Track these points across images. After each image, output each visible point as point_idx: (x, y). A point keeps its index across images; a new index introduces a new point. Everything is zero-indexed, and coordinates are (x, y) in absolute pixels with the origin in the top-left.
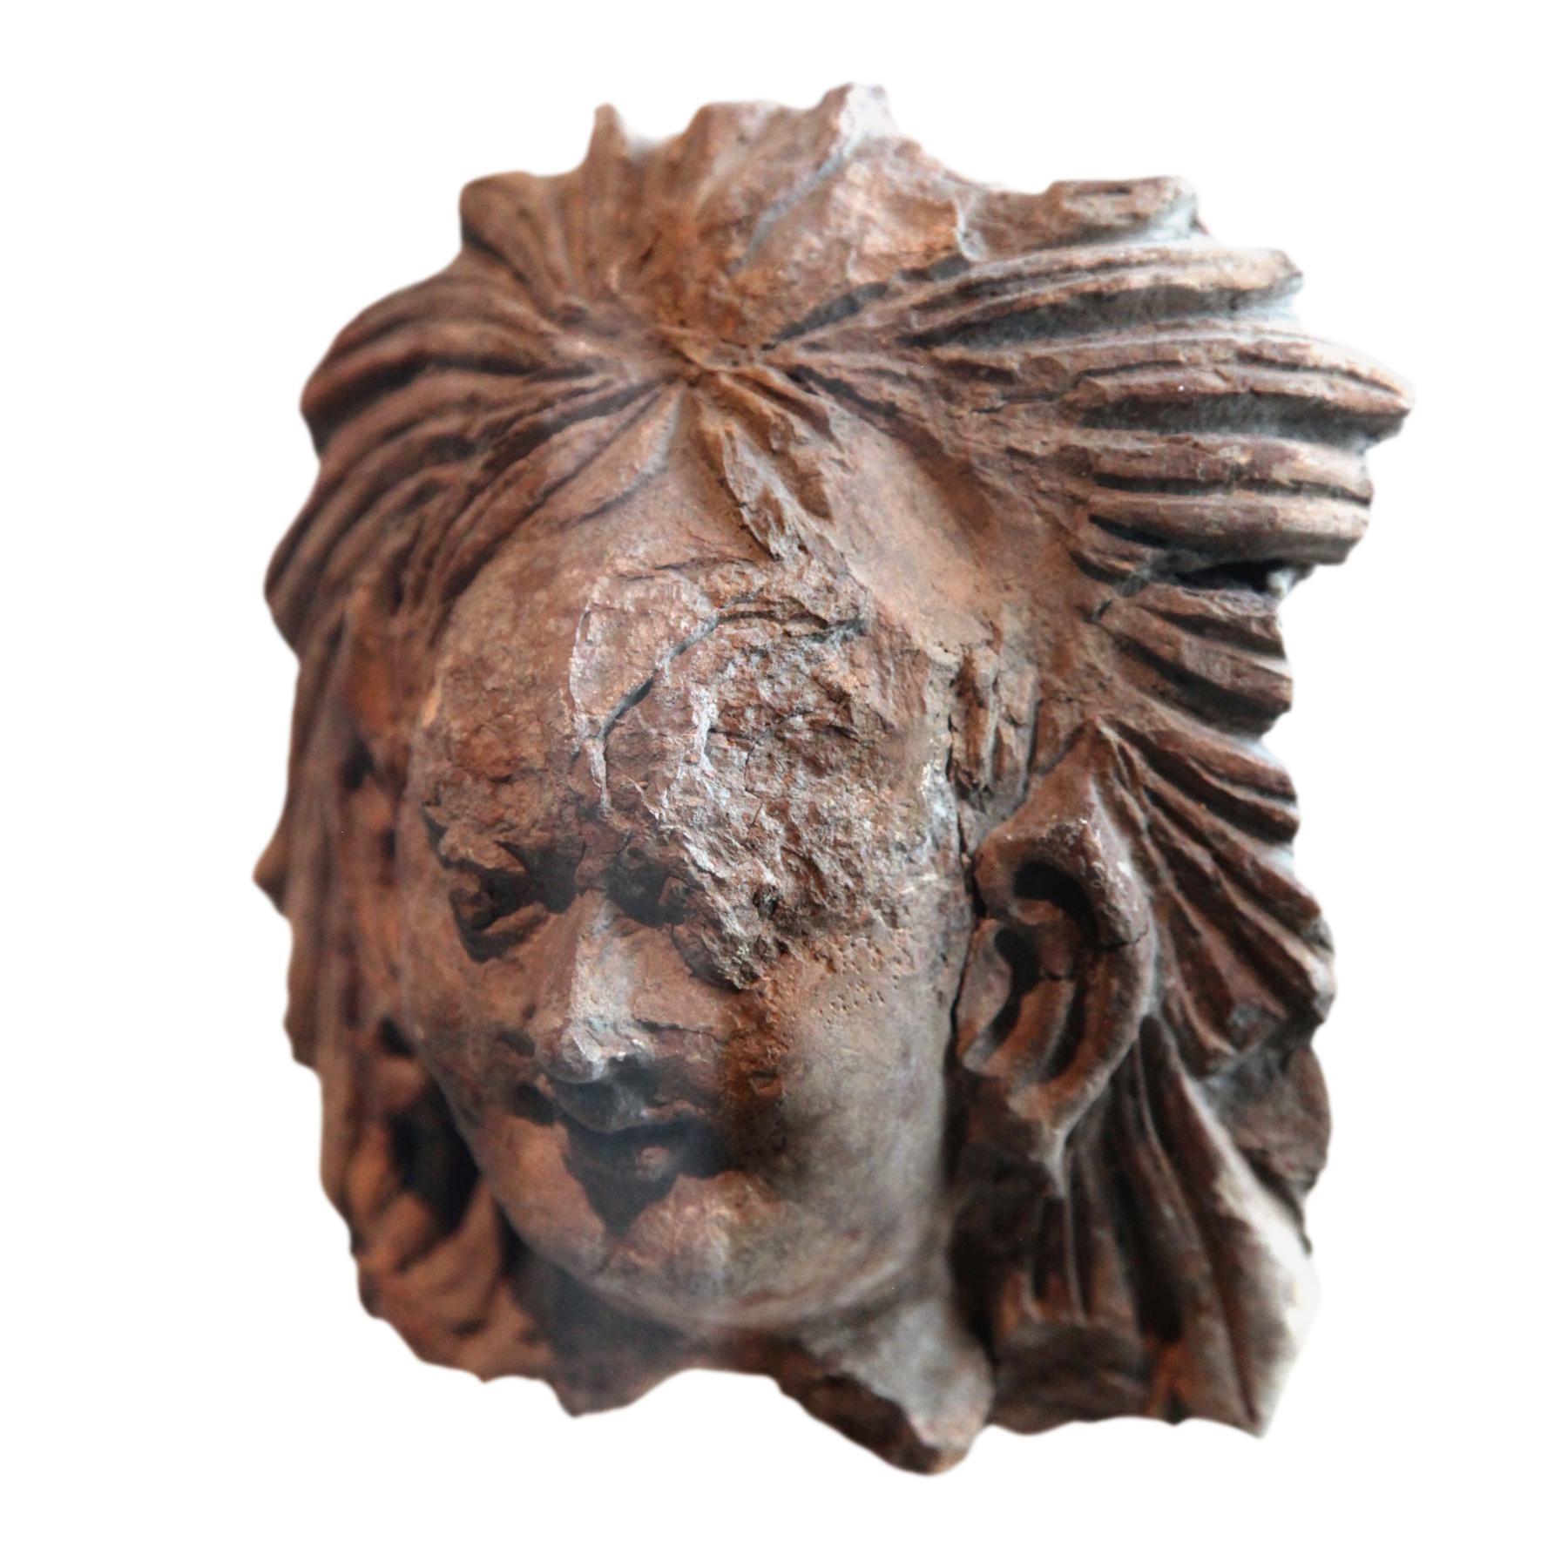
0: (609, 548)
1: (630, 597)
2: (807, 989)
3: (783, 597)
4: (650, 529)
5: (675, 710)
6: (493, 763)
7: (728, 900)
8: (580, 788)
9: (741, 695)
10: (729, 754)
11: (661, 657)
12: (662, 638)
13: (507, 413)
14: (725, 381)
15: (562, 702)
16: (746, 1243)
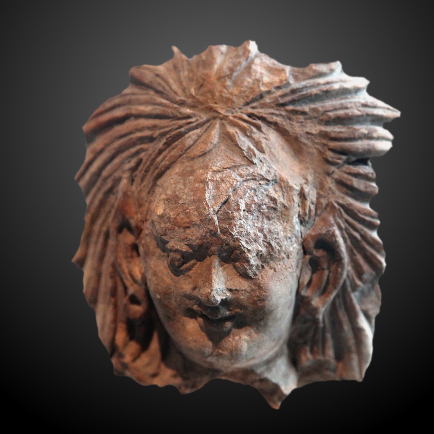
0: (209, 164)
1: (218, 177)
2: (270, 277)
3: (258, 174)
4: (219, 158)
5: (235, 206)
6: (184, 223)
7: (251, 255)
8: (212, 228)
9: (250, 201)
10: (248, 216)
11: (230, 192)
12: (229, 187)
13: (167, 129)
14: (231, 118)
15: (205, 205)
16: (251, 345)
